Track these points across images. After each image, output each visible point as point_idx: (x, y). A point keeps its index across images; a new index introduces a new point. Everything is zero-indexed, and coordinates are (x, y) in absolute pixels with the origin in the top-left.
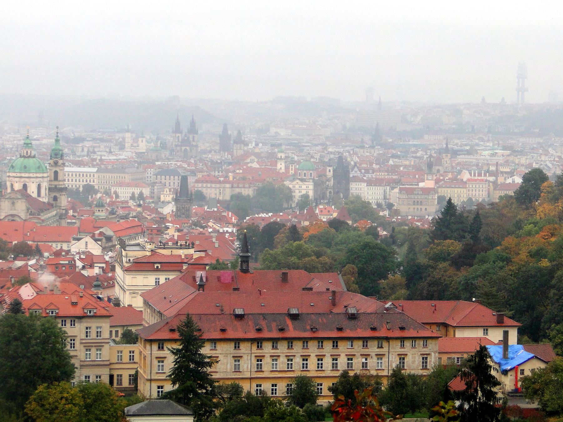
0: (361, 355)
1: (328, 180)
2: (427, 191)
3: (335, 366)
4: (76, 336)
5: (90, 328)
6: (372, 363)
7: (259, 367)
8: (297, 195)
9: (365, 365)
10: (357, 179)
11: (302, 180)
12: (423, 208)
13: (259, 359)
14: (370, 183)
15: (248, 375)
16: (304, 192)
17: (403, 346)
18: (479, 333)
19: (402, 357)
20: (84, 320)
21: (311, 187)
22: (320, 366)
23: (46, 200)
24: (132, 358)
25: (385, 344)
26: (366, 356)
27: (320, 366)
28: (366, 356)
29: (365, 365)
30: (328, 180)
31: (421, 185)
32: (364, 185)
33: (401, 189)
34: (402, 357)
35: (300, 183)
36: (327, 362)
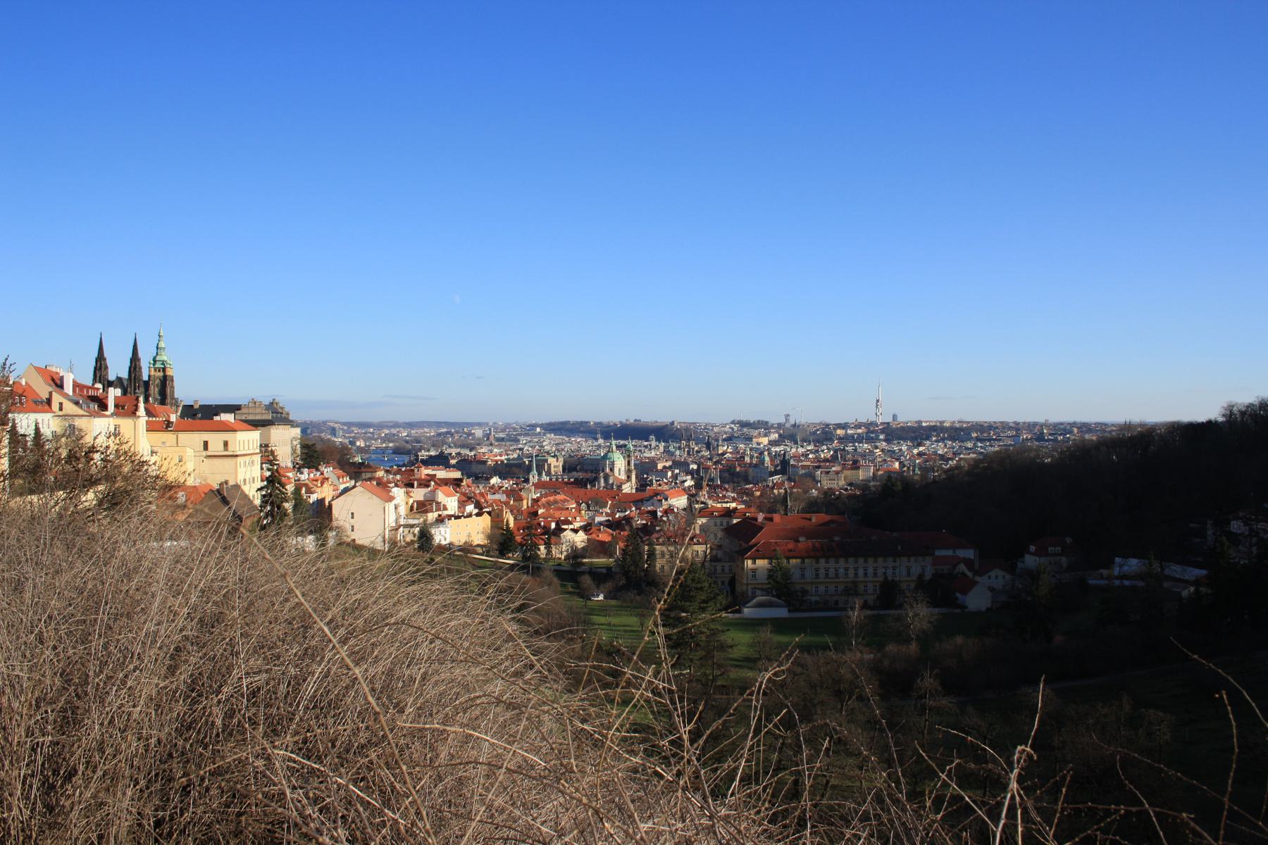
0: (883, 567)
2: (837, 473)
3: (866, 574)
6: (890, 572)
7: (817, 575)
9: (885, 573)
12: (835, 482)
13: (817, 570)
15: (810, 581)
17: (909, 562)
18: (949, 553)
19: (909, 569)
23: (623, 478)
24: (723, 570)
25: (898, 560)
26: (886, 568)
28: (886, 568)
29: (885, 573)
31: (834, 469)
34: (909, 569)
36: (861, 572)
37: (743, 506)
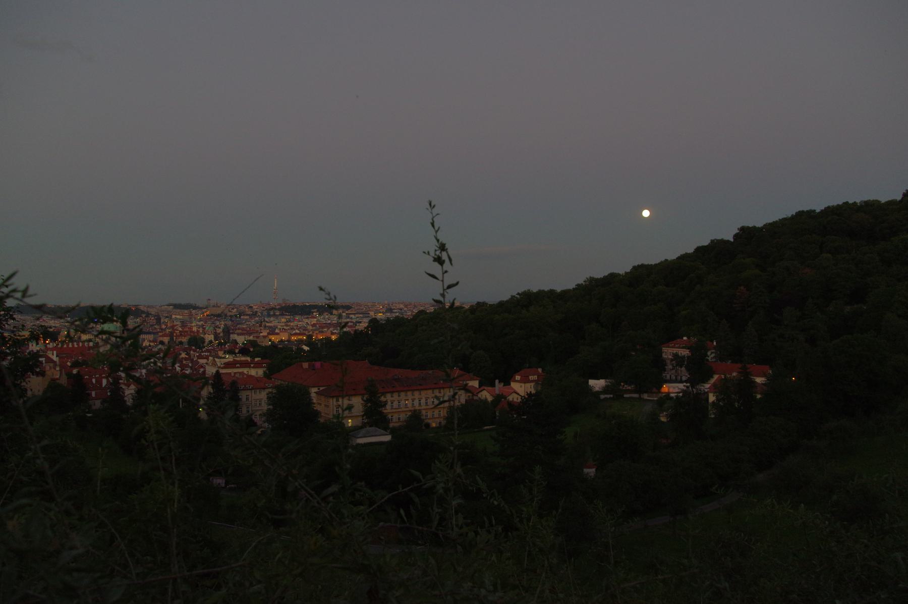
1: (219, 334)
2: (264, 337)
4: (262, 399)
5: (248, 395)
8: (207, 341)
10: (232, 333)
11: (209, 334)
14: (238, 334)
16: (210, 339)
20: (266, 390)
21: (213, 337)
22: (420, 404)
27: (420, 404)
30: (219, 334)
31: (261, 334)
32: (236, 335)
33: (254, 336)
35: (208, 336)
37: (260, 359)
